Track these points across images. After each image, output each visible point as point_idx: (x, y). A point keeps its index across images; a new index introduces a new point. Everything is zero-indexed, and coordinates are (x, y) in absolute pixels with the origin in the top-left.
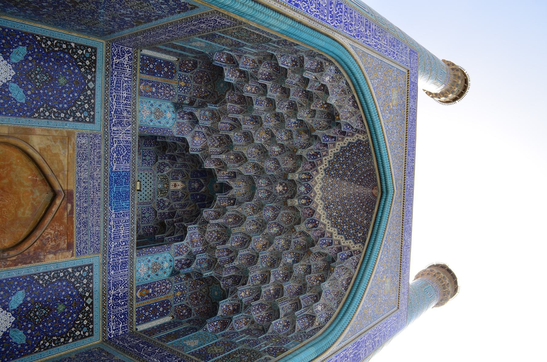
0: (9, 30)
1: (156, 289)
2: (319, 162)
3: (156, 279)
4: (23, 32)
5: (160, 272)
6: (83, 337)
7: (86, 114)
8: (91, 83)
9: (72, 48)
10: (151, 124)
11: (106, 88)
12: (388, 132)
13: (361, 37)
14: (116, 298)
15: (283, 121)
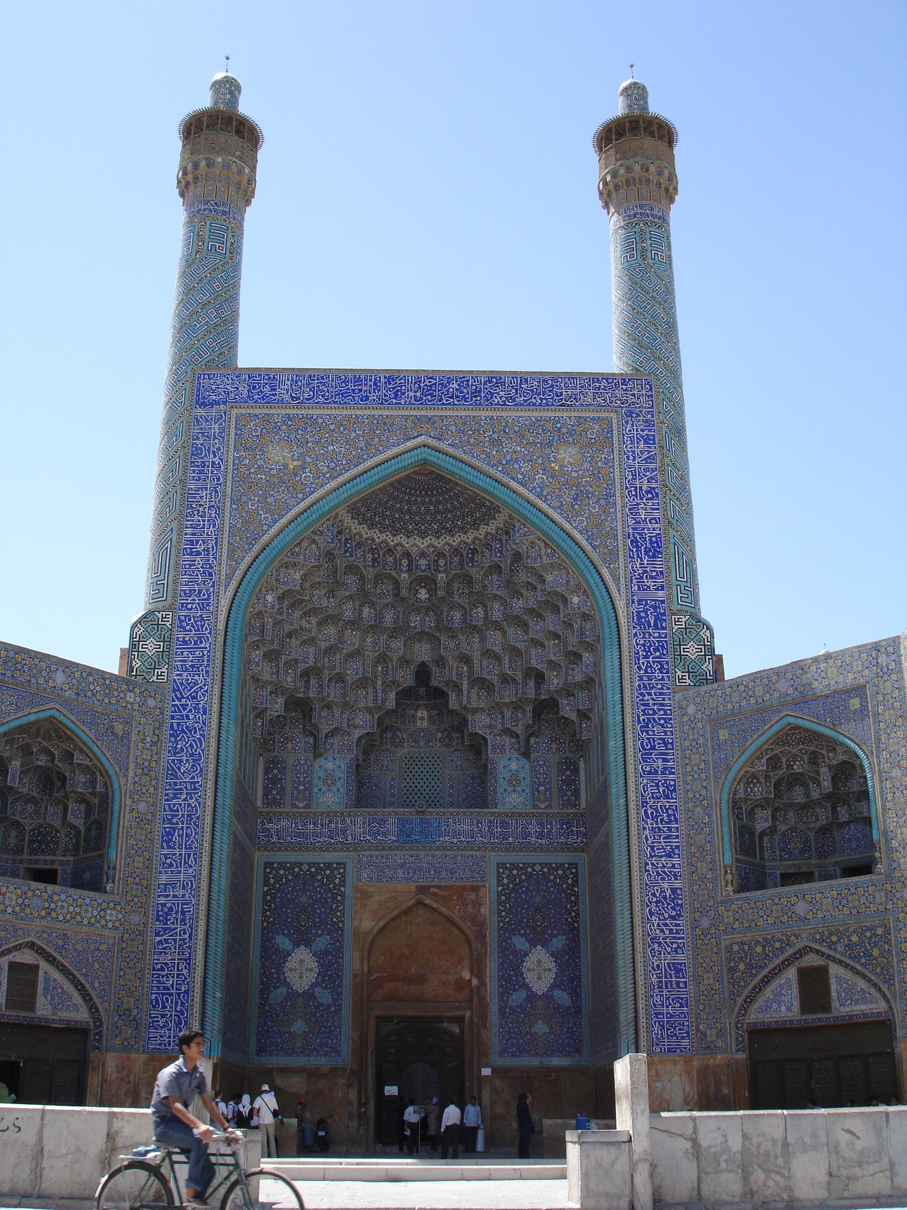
0: (262, 952)
1: (542, 780)
2: (383, 545)
3: (528, 779)
4: (262, 940)
5: (522, 775)
6: (576, 875)
7: (336, 872)
8: (302, 867)
9: (269, 890)
10: (342, 790)
11: (307, 850)
12: (334, 474)
13: (211, 567)
14: (540, 835)
15: (329, 616)
